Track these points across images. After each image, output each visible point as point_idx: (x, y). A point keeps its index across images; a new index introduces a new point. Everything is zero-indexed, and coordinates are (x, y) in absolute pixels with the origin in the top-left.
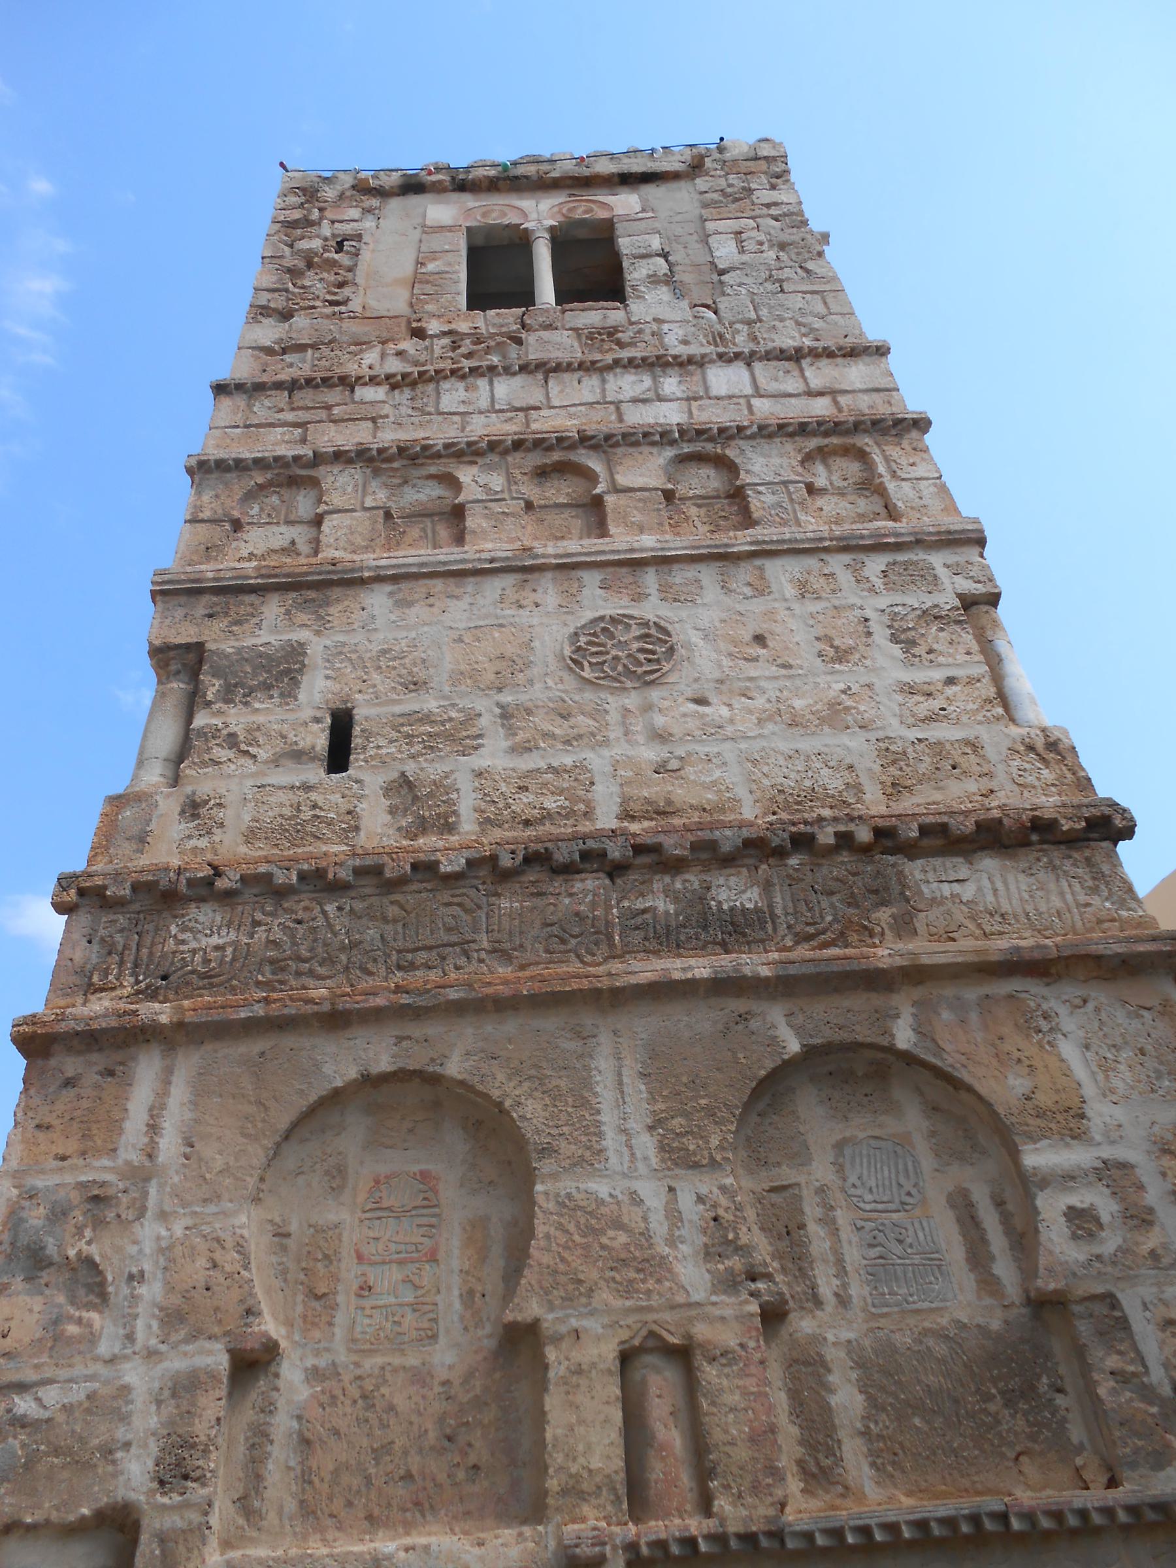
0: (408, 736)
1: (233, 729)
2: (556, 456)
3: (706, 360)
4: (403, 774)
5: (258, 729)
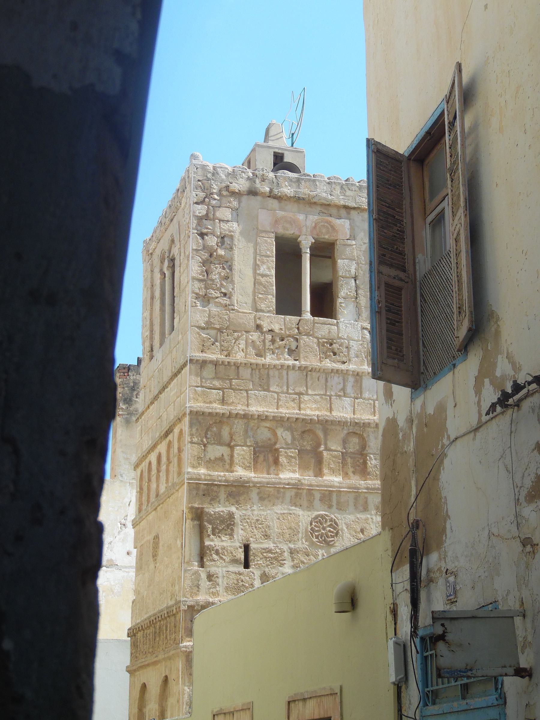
0: (265, 557)
1: (218, 548)
2: (309, 427)
4: (264, 572)
5: (224, 549)
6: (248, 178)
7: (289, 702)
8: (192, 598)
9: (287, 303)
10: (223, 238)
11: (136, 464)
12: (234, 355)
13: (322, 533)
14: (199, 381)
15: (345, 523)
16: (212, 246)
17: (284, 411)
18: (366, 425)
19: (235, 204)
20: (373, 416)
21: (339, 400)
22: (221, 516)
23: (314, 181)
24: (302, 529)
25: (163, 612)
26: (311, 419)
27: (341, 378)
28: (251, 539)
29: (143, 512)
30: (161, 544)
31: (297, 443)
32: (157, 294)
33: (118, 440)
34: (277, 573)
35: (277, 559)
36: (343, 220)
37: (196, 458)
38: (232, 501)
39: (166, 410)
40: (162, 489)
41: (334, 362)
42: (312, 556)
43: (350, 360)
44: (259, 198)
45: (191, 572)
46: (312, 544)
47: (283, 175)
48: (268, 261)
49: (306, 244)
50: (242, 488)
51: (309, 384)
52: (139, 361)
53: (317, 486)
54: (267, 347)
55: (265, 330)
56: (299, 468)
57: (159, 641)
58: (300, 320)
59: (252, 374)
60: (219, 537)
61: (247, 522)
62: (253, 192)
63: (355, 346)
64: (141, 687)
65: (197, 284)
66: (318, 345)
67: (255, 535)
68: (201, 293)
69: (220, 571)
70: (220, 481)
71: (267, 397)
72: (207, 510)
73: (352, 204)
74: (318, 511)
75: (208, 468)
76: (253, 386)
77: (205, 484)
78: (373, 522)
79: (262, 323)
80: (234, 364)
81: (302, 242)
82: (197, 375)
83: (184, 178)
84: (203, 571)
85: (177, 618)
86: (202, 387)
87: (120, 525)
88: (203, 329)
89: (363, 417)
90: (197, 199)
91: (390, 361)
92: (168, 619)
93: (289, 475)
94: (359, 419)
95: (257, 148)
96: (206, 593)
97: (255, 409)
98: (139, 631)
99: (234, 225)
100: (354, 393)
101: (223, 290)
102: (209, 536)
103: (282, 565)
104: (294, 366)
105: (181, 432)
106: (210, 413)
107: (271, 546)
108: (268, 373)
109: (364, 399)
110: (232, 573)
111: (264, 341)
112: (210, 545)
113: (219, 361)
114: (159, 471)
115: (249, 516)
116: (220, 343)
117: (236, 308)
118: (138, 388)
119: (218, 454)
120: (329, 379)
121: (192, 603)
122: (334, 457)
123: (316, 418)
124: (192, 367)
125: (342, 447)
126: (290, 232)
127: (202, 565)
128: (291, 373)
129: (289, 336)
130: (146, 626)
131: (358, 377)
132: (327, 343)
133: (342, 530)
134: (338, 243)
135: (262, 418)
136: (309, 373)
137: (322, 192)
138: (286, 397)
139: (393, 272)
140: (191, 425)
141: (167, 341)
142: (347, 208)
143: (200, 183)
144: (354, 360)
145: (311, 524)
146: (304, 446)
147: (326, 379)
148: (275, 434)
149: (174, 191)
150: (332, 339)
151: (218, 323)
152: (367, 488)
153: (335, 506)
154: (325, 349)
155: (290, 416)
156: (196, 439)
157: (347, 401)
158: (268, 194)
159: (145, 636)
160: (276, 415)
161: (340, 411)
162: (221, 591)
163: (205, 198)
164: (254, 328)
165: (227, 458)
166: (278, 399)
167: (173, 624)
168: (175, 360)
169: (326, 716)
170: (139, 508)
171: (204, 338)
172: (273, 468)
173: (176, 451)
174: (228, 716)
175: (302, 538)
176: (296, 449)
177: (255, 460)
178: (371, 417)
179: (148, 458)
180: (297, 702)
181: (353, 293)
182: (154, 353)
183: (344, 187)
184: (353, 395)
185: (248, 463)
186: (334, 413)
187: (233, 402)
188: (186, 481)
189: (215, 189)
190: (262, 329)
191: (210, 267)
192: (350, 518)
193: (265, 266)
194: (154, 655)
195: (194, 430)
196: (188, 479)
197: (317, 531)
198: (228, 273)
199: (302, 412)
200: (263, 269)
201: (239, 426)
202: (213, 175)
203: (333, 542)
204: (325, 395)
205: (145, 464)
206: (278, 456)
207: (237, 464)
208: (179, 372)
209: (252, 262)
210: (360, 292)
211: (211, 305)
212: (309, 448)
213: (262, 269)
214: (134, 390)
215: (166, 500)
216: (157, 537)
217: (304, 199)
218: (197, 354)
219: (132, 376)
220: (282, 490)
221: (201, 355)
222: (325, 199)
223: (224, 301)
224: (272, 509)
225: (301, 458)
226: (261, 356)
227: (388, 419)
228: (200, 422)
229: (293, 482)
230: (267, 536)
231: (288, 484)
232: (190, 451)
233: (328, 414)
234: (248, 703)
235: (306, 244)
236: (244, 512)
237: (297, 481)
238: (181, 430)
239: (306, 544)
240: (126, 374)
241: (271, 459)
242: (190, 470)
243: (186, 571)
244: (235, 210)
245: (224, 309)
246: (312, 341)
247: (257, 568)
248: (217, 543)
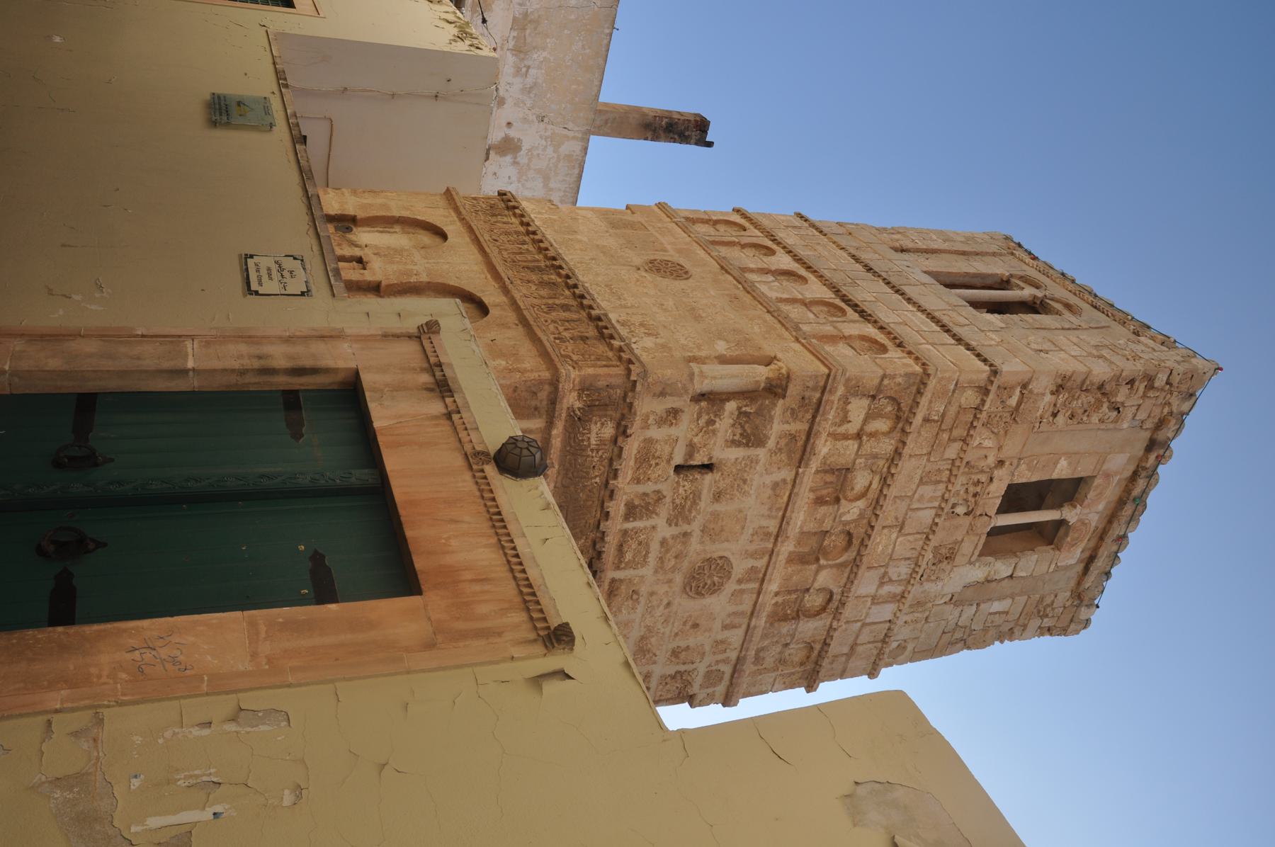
1: (717, 425)
2: (856, 542)
18: (836, 615)
35: (681, 514)
38: (783, 442)
39: (877, 300)
44: (1141, 453)
50: (798, 456)
51: (910, 538)
62: (1151, 445)
66: (956, 542)
93: (800, 519)
103: (669, 522)
105: (884, 349)
107: (702, 505)
111: (982, 472)
119: (851, 416)
124: (985, 376)
128: (933, 512)
137: (1117, 530)
140: (907, 375)
148: (858, 498)
153: (738, 587)
159: (522, 238)
164: (1002, 456)
165: (842, 430)
195: (900, 380)
200: (1063, 463)
201: (887, 446)
208: (959, 340)
212: (826, 543)
219: (695, 135)
220: (781, 514)
230: (718, 497)
235: (1070, 514)
238: (884, 349)
241: (824, 492)
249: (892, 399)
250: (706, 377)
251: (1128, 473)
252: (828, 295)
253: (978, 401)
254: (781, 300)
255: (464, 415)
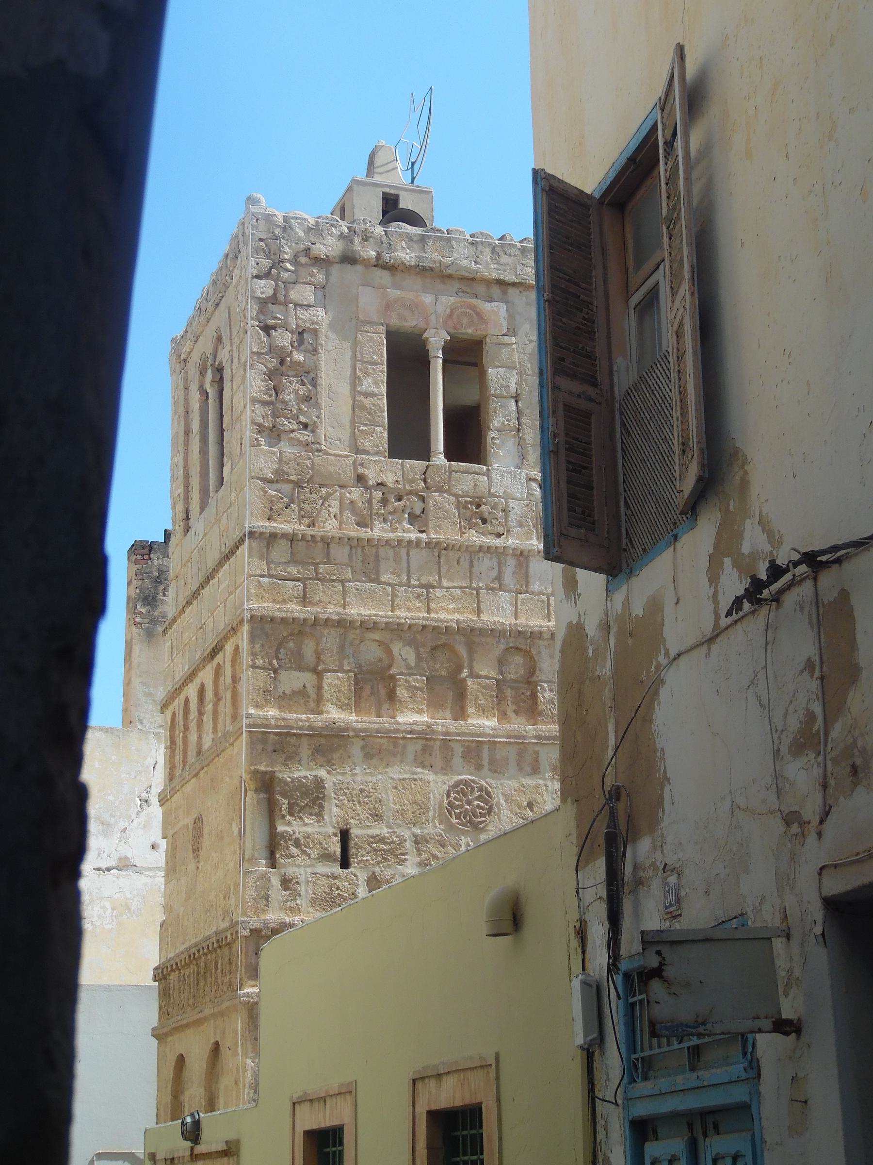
0: (375, 850)
1: (297, 836)
2: (443, 639)
3: (531, 554)
4: (374, 873)
5: (308, 837)
6: (342, 236)
7: (414, 1081)
8: (258, 916)
9: (407, 440)
10: (301, 334)
11: (164, 702)
12: (322, 524)
13: (466, 809)
14: (265, 567)
15: (503, 794)
16: (283, 347)
17: (402, 614)
18: (535, 636)
19: (320, 277)
20: (546, 620)
21: (491, 596)
22: (302, 785)
23: (449, 240)
24: (433, 803)
25: (211, 941)
26: (446, 627)
27: (494, 559)
28: (352, 821)
29: (176, 781)
30: (206, 831)
31: (425, 665)
32: (195, 426)
33: (134, 664)
34: (395, 875)
35: (393, 852)
36: (496, 304)
37: (261, 691)
38: (320, 759)
40: (207, 742)
41: (483, 534)
42: (450, 848)
43: (508, 531)
44: (359, 268)
45: (256, 876)
46: (451, 827)
47: (397, 230)
48: (374, 370)
49: (436, 343)
50: (336, 740)
51: (443, 571)
52: (167, 534)
53: (458, 734)
54: (374, 511)
55: (371, 483)
56: (428, 705)
57: (204, 986)
58: (427, 467)
59: (350, 556)
60: (300, 818)
61: (346, 795)
63: (517, 508)
64: (177, 1061)
65: (260, 410)
66: (458, 505)
67: (358, 815)
68: (266, 424)
69: (303, 873)
70: (301, 728)
71: (375, 592)
72: (280, 775)
73: (511, 278)
74: (459, 775)
75: (280, 708)
76: (352, 574)
77: (276, 734)
78: (547, 791)
79: (367, 472)
80: (322, 539)
81: (431, 339)
82: (261, 557)
83: (237, 237)
84: (275, 873)
85: (234, 949)
86: (270, 576)
87: (139, 802)
88: (271, 482)
89: (531, 623)
90: (258, 270)
91: (573, 532)
92: (219, 950)
93: (410, 718)
94: (523, 626)
95: (355, 187)
96: (280, 909)
97: (357, 611)
98: (172, 970)
99: (319, 313)
100: (515, 585)
101: (302, 419)
102: (283, 817)
103: (402, 862)
104: (418, 542)
105: (237, 647)
106: (282, 619)
107: (385, 831)
108: (377, 552)
109: (533, 593)
110: (323, 876)
111: (370, 502)
112: (286, 832)
113: (297, 534)
114: (201, 713)
115: (348, 783)
116: (299, 505)
117: (323, 447)
118: (166, 579)
119: (297, 685)
120: (475, 562)
121: (257, 926)
122: (484, 687)
123: (454, 625)
124: (254, 544)
125: (497, 671)
126: (410, 323)
127: (273, 864)
128: (414, 552)
129: (411, 493)
130: (183, 963)
131: (522, 559)
132: (471, 503)
133: (498, 804)
134: (488, 340)
135: (367, 626)
136: (443, 552)
137: (462, 259)
138: (406, 592)
139: (576, 387)
140: (252, 639)
141: (212, 502)
142: (501, 283)
143: (262, 244)
144: (515, 530)
145: (448, 796)
146: (437, 671)
147: (471, 562)
148: (389, 652)
149: (221, 256)
150: (480, 498)
151: (293, 472)
152: (538, 737)
154: (468, 513)
155: (413, 622)
156: (261, 661)
157: (505, 597)
158: (373, 262)
159: (182, 978)
160: (391, 620)
161: (493, 614)
162: (304, 905)
163: (271, 268)
165: (311, 691)
166: (394, 596)
167: (226, 960)
168: (225, 534)
169: (474, 1102)
170: (170, 774)
171: (273, 496)
172: (386, 706)
173: (229, 680)
174: (316, 1104)
175: (434, 818)
176: (422, 675)
177: (358, 693)
178: (544, 623)
179: (184, 692)
180: (427, 1080)
181: (514, 423)
182: (192, 522)
183: (497, 249)
184: (513, 588)
185: (345, 699)
186: (484, 617)
187: (320, 601)
188: (244, 729)
189: (286, 253)
190: (366, 482)
191: (281, 382)
192: (511, 784)
193: (370, 380)
194: (197, 1010)
195: (258, 646)
196: (249, 726)
197: (458, 807)
198: (310, 391)
199: (432, 615)
200: (367, 384)
201: (330, 639)
202: (284, 230)
203: (484, 824)
204: (470, 588)
205: (178, 703)
206: (394, 687)
207: (328, 701)
208: (232, 552)
209: (349, 374)
210: (524, 420)
211: (282, 443)
212: (443, 674)
213: (365, 383)
214: (160, 583)
215: (213, 759)
216: (199, 820)
217: (431, 269)
218: (261, 524)
219: (156, 561)
220: (401, 742)
221: (268, 524)
222: (466, 269)
223: (305, 436)
224: (386, 773)
225: (430, 690)
226: (366, 526)
227: (570, 625)
228: (267, 635)
229: (419, 728)
230: (377, 816)
231: (411, 732)
232: (251, 680)
233: (475, 618)
234: (350, 1083)
235: (436, 343)
236: (340, 777)
237: (424, 728)
238: (237, 647)
239: (440, 828)
240: (146, 557)
241: (383, 692)
242: (252, 711)
243: (246, 873)
244: (321, 288)
245: (304, 449)
246: (446, 502)
247: (361, 867)
248: (296, 829)
249: (280, 646)
250: (253, 855)
251: (384, 277)
252: (210, 669)
253: (283, 542)
254: (215, 728)
255: (181, 1155)
